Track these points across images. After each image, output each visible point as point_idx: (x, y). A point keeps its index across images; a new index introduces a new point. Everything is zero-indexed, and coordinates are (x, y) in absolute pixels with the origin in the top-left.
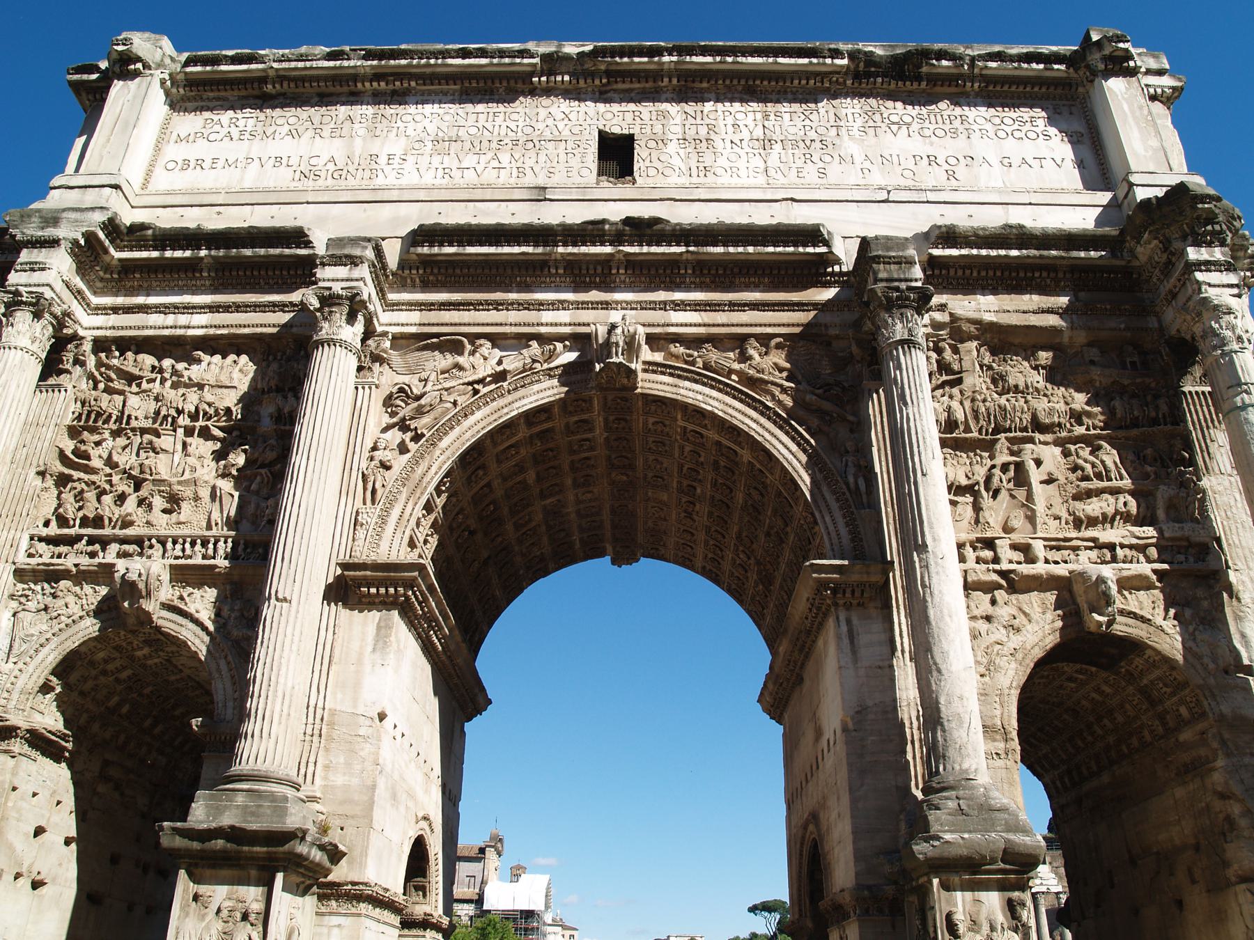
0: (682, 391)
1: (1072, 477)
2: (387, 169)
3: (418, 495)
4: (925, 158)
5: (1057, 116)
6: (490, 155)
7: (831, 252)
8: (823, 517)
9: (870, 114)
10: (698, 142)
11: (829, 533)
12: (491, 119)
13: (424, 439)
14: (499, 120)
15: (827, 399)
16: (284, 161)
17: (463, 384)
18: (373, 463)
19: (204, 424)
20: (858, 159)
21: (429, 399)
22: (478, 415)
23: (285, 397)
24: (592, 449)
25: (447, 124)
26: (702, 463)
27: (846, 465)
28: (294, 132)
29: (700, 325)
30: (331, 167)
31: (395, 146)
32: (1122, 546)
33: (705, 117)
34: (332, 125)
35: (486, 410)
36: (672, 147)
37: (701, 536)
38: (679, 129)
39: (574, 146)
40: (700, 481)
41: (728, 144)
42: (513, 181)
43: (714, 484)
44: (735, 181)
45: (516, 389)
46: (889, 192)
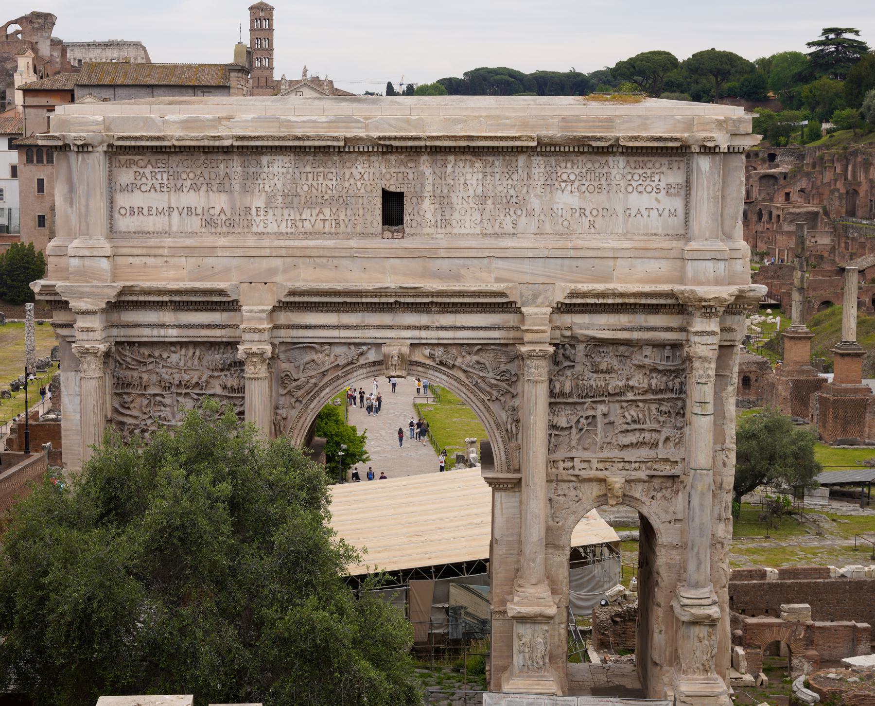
1: (622, 420)
2: (258, 219)
5: (669, 171)
14: (321, 179)
15: (503, 381)
16: (193, 210)
18: (279, 418)
19: (187, 391)
20: (537, 212)
22: (327, 390)
23: (226, 376)
30: (222, 215)
31: (259, 202)
32: (635, 462)
35: (331, 387)
38: (429, 188)
42: (333, 230)
44: (463, 231)
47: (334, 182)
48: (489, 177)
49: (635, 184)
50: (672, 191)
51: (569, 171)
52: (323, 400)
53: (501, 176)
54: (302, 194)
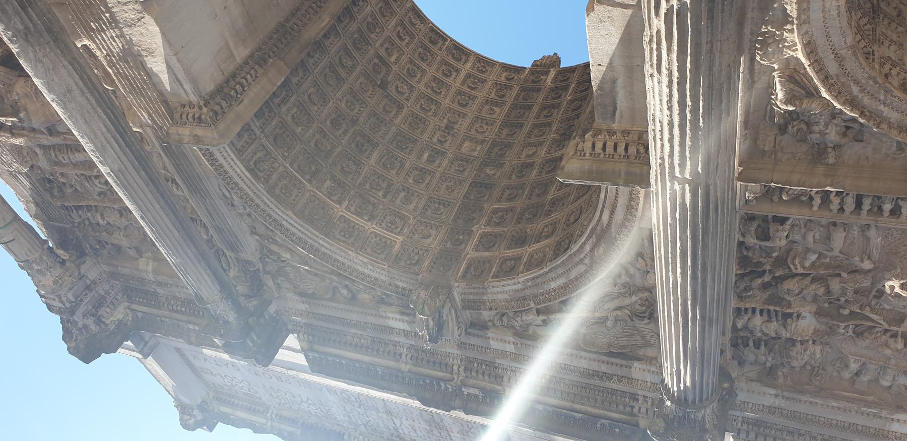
3: (599, 228)
24: (495, 211)
26: (404, 190)
35: (546, 288)
40: (416, 169)
45: (524, 299)
48: (392, 429)
52: (560, 271)
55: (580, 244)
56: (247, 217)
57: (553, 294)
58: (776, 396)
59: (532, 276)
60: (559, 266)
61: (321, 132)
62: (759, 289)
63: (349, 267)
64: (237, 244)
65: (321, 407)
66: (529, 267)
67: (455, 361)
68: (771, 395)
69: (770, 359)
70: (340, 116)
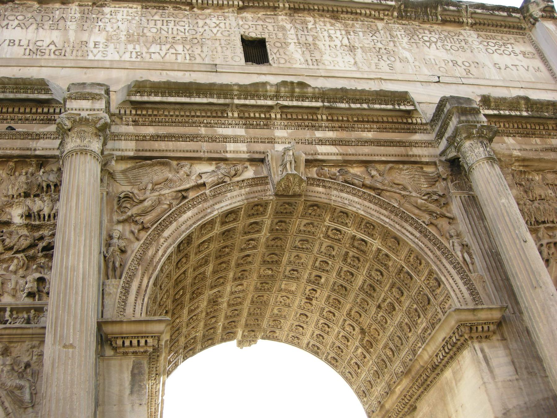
0: (333, 198)
3: (151, 272)
4: (450, 62)
6: (168, 46)
7: (416, 110)
8: (447, 279)
9: (411, 35)
10: (308, 45)
11: (454, 291)
12: (165, 24)
13: (151, 230)
14: (171, 25)
15: (431, 203)
16: (17, 42)
17: (177, 191)
18: (111, 249)
20: (411, 60)
21: (150, 202)
22: (189, 214)
24: (254, 247)
25: (135, 25)
26: (333, 256)
27: (453, 245)
28: (22, 25)
29: (337, 154)
30: (53, 47)
33: (309, 31)
34: (51, 22)
35: (195, 210)
36: (292, 48)
37: (314, 317)
38: (294, 37)
39: (226, 43)
40: (327, 271)
41: (328, 47)
43: (339, 274)
45: (214, 196)
46: (439, 77)
47: (187, 28)
48: (352, 33)
49: (494, 49)
50: (527, 56)
51: (429, 36)
52: (184, 227)
53: (363, 34)
54: (148, 34)
55: (165, 255)
56: (453, 234)
57: (190, 206)
58: (35, 150)
59: (207, 218)
60: (184, 232)
61: (400, 302)
62: (45, 237)
63: (365, 199)
64: (468, 205)
65: (418, 41)
66: (212, 222)
67: (279, 123)
68: (39, 150)
69: (40, 178)
70: (389, 313)
